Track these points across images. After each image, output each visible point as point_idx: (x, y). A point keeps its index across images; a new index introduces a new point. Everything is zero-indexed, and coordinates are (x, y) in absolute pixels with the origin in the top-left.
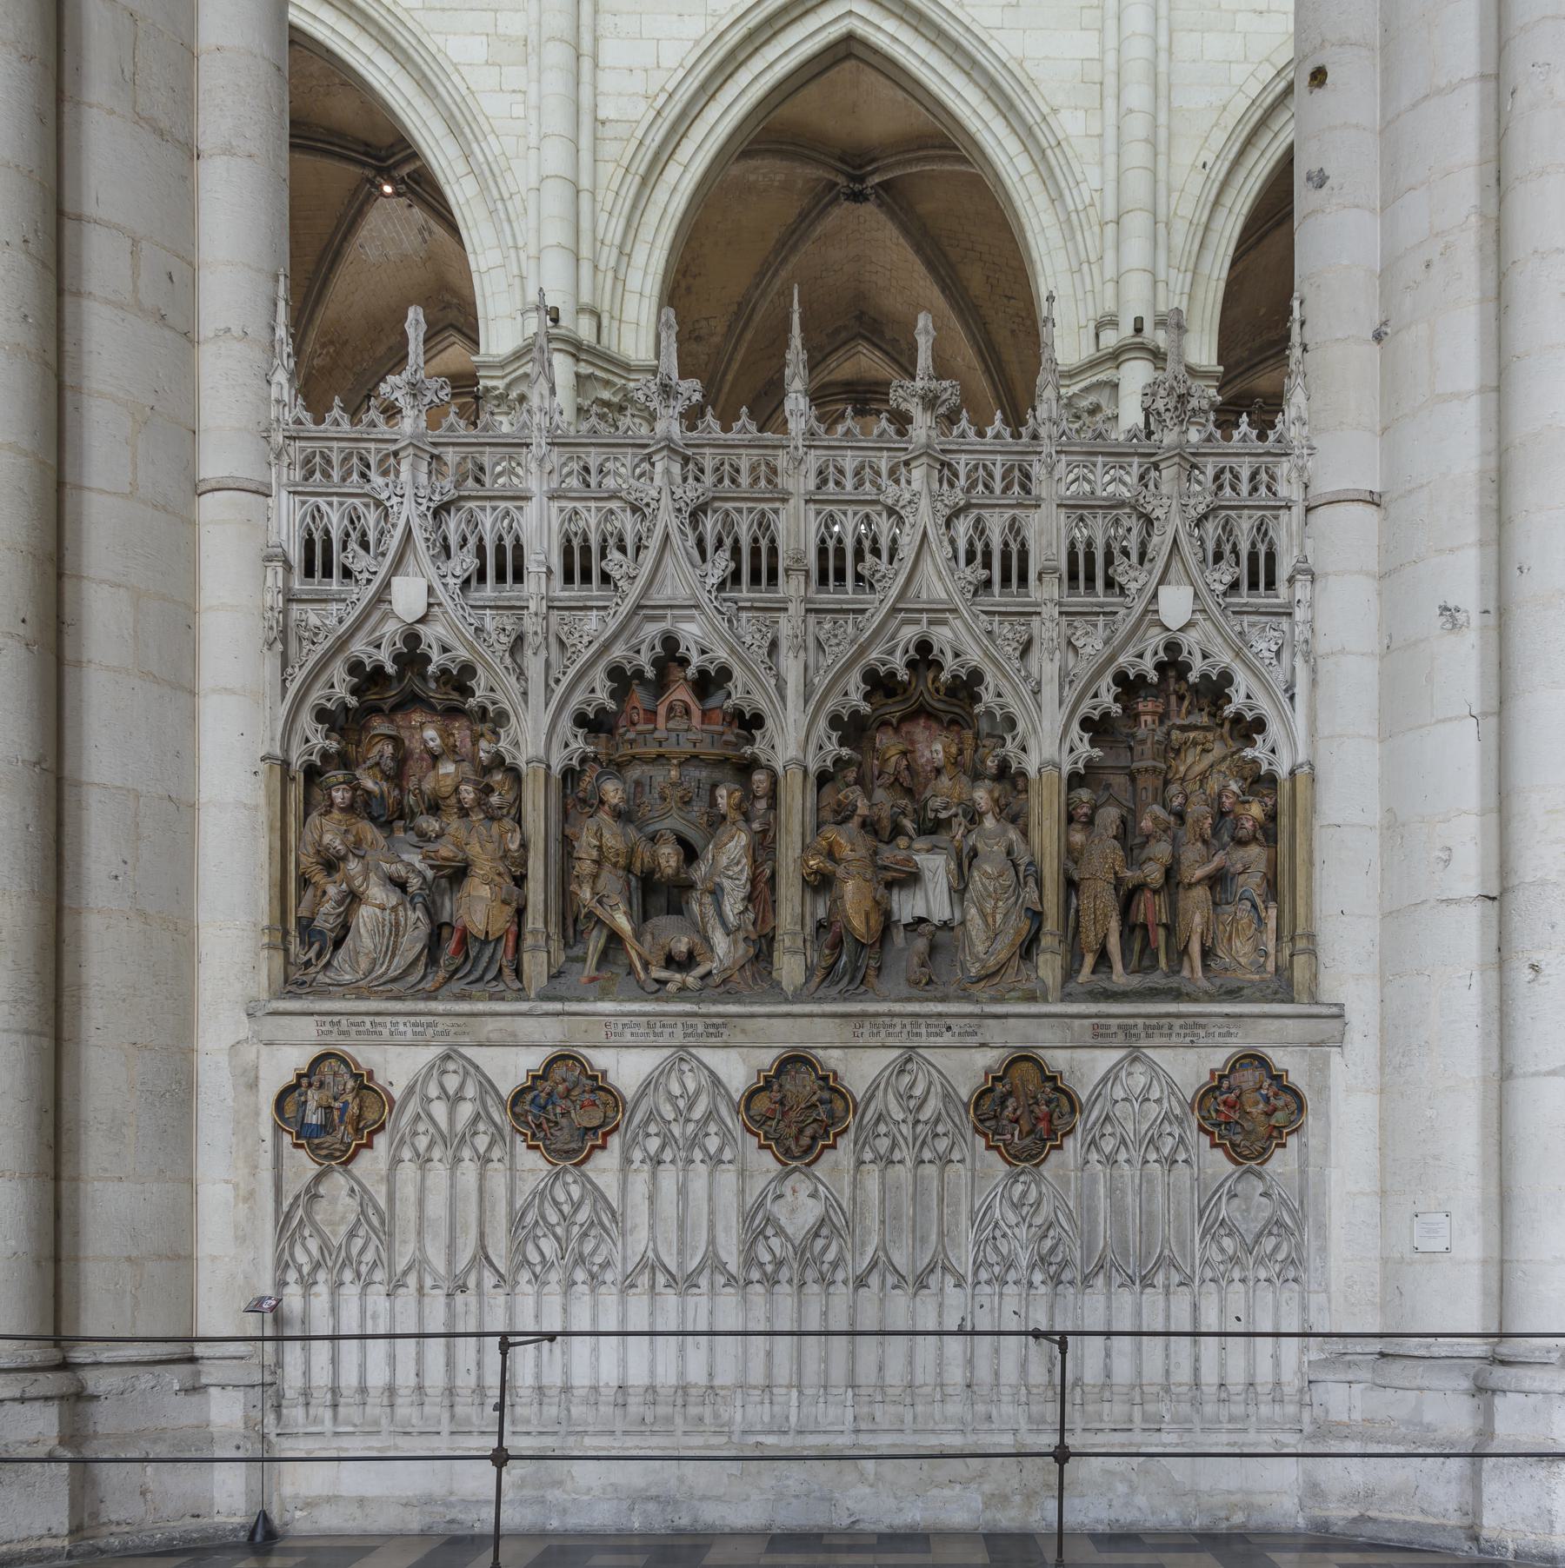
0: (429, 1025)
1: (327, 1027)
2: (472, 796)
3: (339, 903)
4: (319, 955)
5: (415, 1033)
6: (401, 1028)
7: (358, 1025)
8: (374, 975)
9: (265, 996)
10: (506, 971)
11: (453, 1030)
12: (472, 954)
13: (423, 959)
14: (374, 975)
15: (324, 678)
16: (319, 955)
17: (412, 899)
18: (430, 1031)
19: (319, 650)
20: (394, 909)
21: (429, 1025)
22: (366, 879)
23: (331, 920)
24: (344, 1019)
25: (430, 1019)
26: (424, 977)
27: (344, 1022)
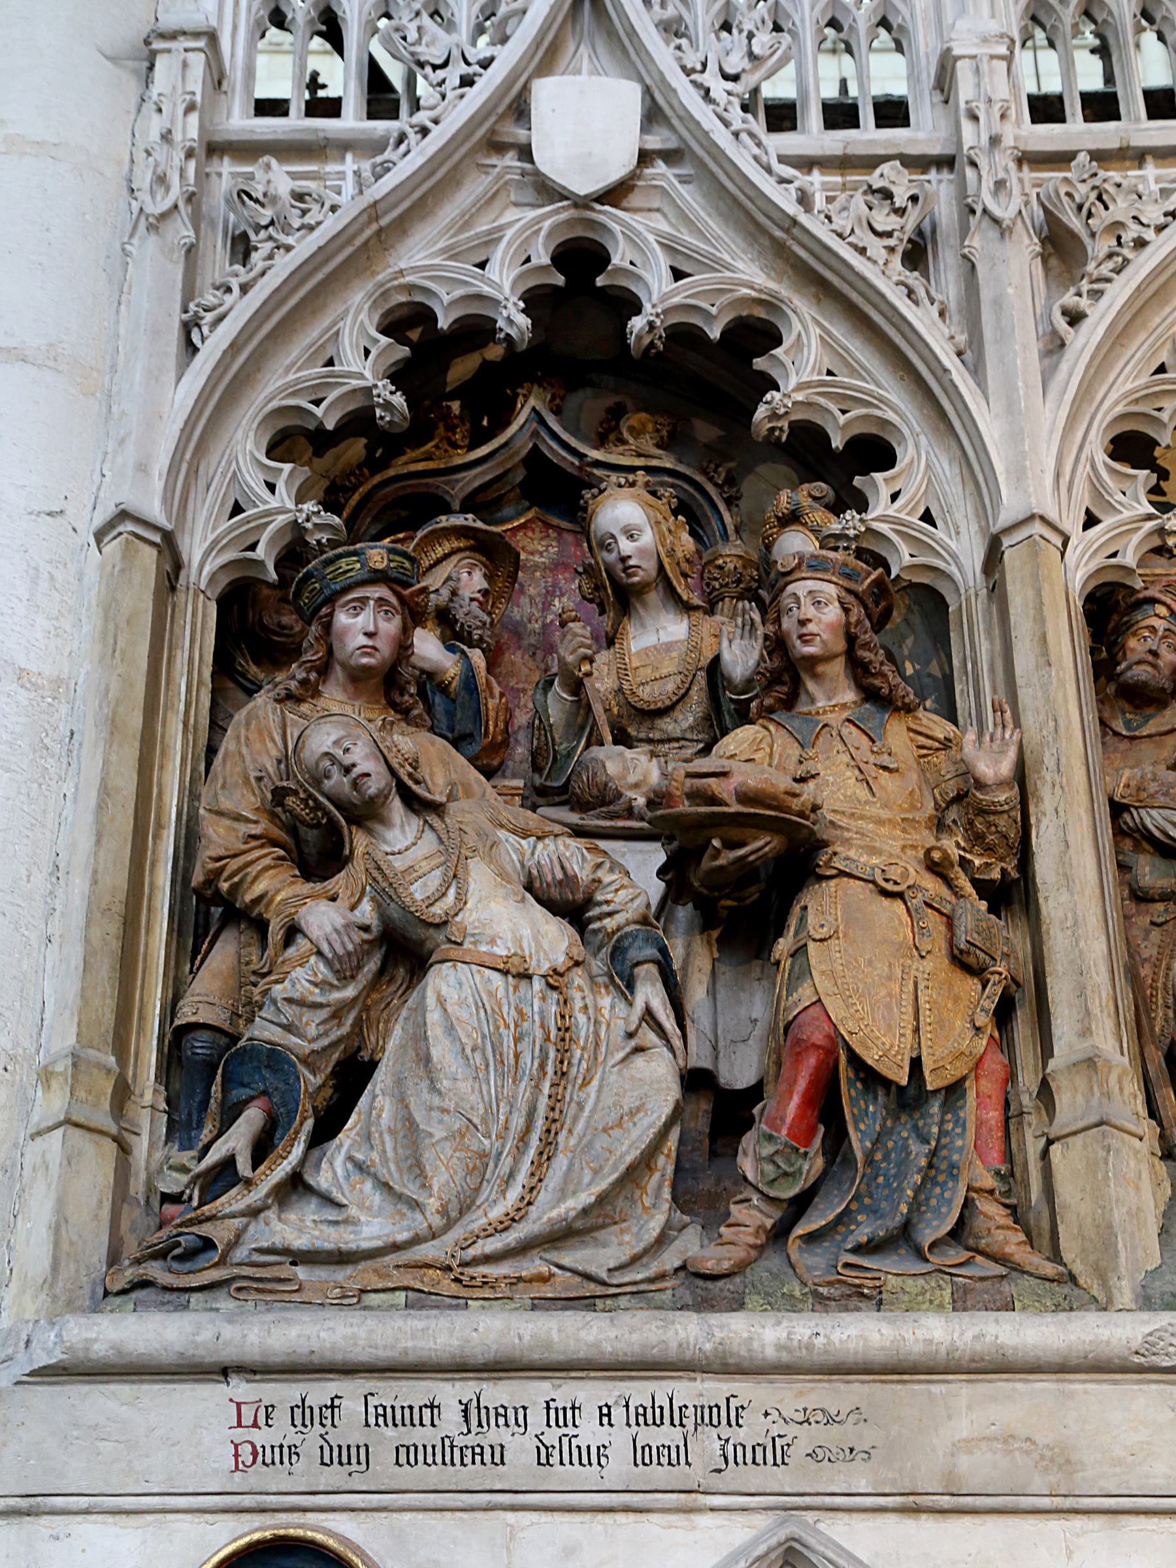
0: (708, 1416)
1: (280, 1432)
2: (833, 613)
3: (344, 969)
4: (262, 1149)
5: (642, 1455)
6: (589, 1432)
7: (409, 1417)
8: (477, 1221)
9: (32, 1306)
10: (991, 1210)
11: (804, 1439)
12: (858, 1143)
13: (665, 1164)
14: (477, 1221)
15: (312, 334)
16: (262, 1149)
17: (618, 952)
18: (707, 1444)
19: (305, 247)
20: (555, 981)
21: (708, 1416)
22: (455, 877)
23: (312, 1023)
24: (351, 1392)
25: (713, 1389)
26: (662, 1241)
27: (351, 1406)
